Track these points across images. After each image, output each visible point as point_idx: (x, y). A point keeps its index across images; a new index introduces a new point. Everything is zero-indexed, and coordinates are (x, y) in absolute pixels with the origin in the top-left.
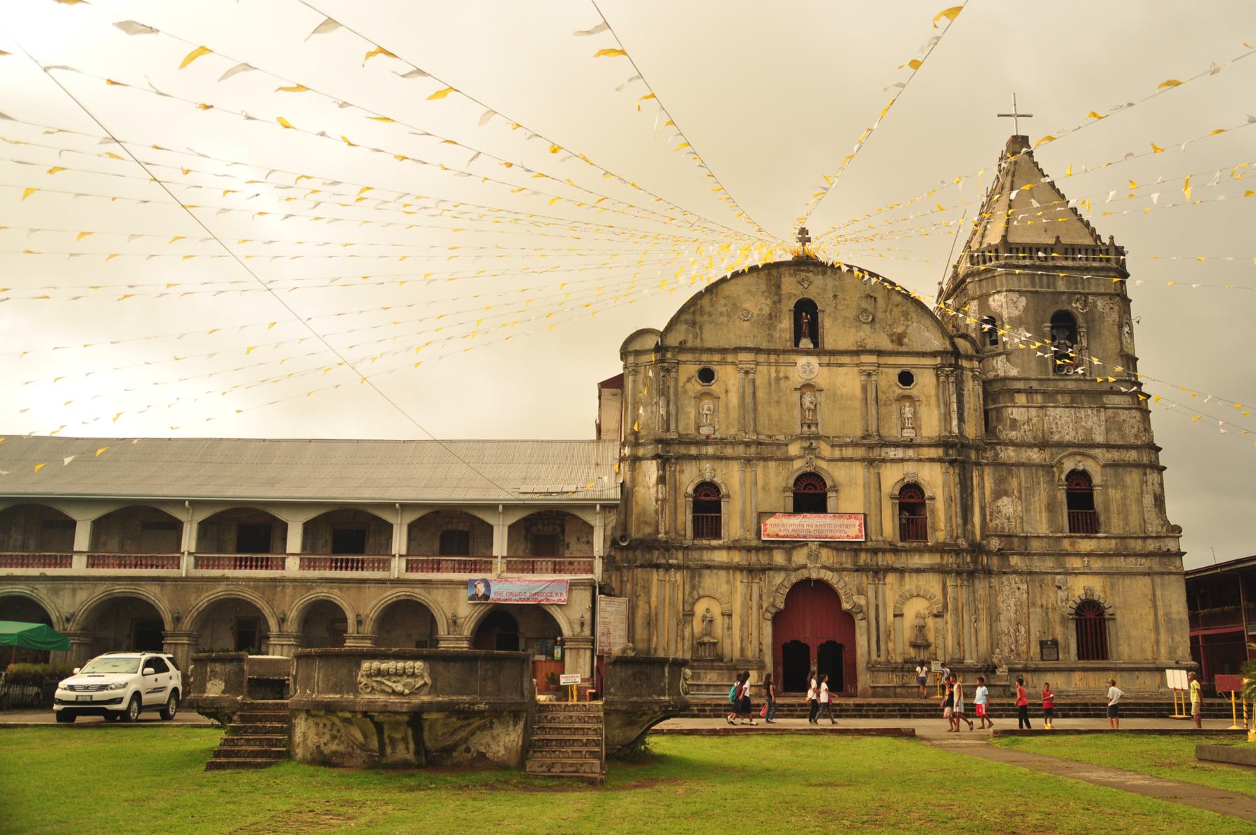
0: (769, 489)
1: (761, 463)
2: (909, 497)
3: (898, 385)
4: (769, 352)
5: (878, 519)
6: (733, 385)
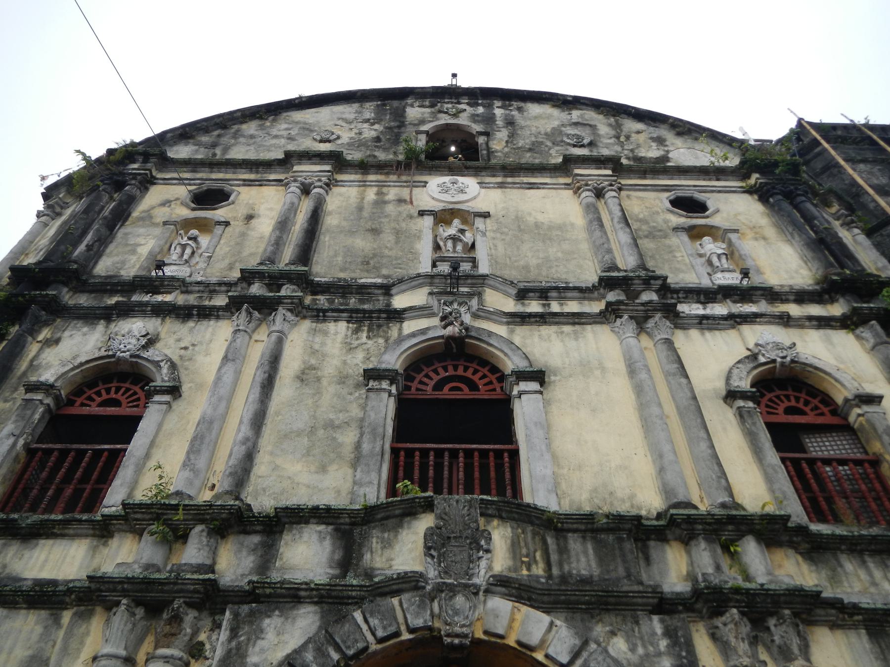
0: (319, 379)
1: (307, 324)
2: (789, 411)
3: (671, 212)
4: (364, 167)
5: (704, 445)
6: (271, 209)
